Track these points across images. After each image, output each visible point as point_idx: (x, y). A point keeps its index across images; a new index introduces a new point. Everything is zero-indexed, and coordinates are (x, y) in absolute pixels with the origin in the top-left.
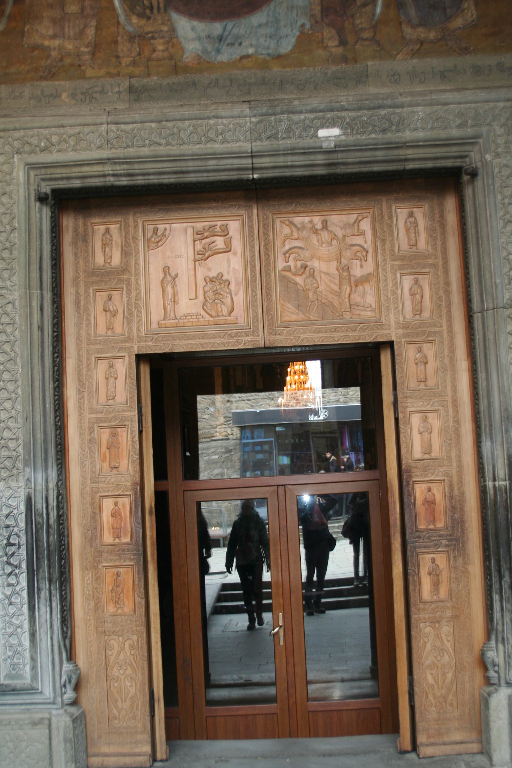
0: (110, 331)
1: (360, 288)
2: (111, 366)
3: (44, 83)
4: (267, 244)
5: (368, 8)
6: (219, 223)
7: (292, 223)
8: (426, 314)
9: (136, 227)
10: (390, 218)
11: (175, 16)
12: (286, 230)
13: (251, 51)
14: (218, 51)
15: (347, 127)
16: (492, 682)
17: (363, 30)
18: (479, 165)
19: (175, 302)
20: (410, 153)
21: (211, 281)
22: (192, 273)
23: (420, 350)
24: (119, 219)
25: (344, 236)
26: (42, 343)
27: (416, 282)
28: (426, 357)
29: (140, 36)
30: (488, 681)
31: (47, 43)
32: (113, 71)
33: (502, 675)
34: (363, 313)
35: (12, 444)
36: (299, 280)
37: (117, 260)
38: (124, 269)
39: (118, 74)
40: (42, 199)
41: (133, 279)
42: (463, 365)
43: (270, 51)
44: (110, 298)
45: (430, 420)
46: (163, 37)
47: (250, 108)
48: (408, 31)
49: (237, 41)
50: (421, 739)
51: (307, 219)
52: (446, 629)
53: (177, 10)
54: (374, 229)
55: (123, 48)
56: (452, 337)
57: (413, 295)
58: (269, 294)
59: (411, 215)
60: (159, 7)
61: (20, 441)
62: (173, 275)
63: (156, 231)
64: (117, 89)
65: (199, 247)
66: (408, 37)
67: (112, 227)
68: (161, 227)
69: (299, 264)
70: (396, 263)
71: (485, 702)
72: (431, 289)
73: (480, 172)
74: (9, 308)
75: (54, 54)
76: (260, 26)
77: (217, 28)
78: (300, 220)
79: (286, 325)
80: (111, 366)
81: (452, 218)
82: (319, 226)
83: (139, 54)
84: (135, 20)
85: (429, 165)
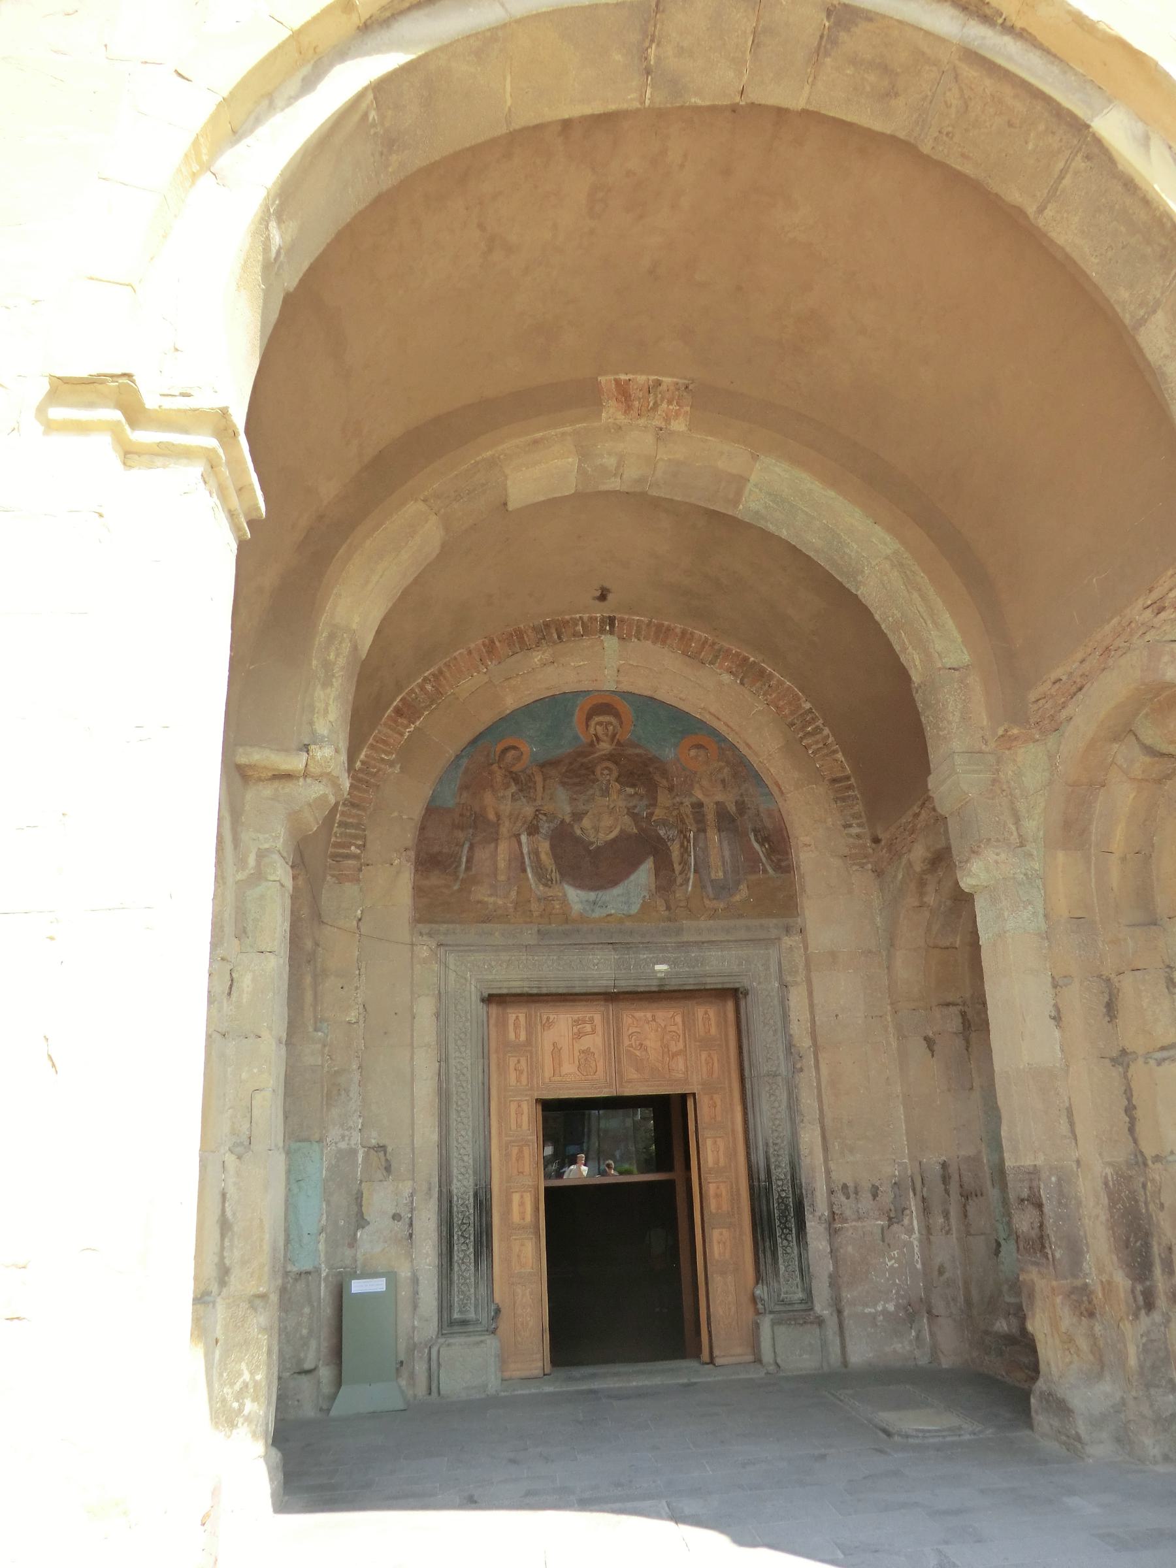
0: (518, 1084)
1: (675, 1058)
2: (519, 1106)
3: (484, 925)
4: (618, 1029)
5: (684, 887)
6: (588, 1015)
7: (633, 1016)
8: (715, 1075)
9: (536, 1016)
10: (694, 1014)
11: (566, 886)
12: (630, 1021)
13: (613, 912)
14: (593, 911)
15: (673, 963)
16: (760, 1311)
17: (680, 900)
18: (749, 988)
19: (560, 1065)
20: (709, 980)
21: (583, 1052)
22: (571, 1047)
23: (712, 1099)
24: (525, 1010)
25: (665, 1026)
26: (484, 1093)
27: (709, 1055)
28: (715, 1103)
29: (545, 898)
30: (758, 1313)
31: (486, 899)
32: (529, 920)
33: (766, 1306)
34: (677, 1075)
35: (466, 1158)
36: (638, 1053)
37: (523, 1037)
38: (529, 1042)
39: (531, 922)
40: (483, 1000)
41: (534, 1049)
42: (738, 1109)
43: (625, 912)
44: (519, 1062)
45: (718, 1143)
46: (558, 900)
47: (614, 949)
48: (707, 902)
49: (604, 906)
50: (716, 1352)
51: (642, 1014)
52: (730, 1278)
53: (568, 883)
54: (683, 1022)
55: (534, 906)
56: (731, 1091)
57: (707, 1064)
58: (619, 1062)
59: (706, 1013)
60: (556, 881)
61: (471, 1156)
62: (559, 1048)
63: (548, 1019)
64: (529, 932)
65: (575, 1030)
66: (707, 906)
67: (520, 1015)
68: (552, 1017)
69: (638, 1043)
70: (698, 1043)
71: (757, 1326)
72: (718, 1061)
73: (750, 993)
74: (465, 1071)
75: (491, 907)
76: (618, 895)
77: (592, 895)
78: (639, 1014)
79: (629, 1081)
80: (519, 1106)
81: (731, 1015)
82: (650, 1019)
83: (544, 910)
84: (541, 888)
85: (720, 986)
